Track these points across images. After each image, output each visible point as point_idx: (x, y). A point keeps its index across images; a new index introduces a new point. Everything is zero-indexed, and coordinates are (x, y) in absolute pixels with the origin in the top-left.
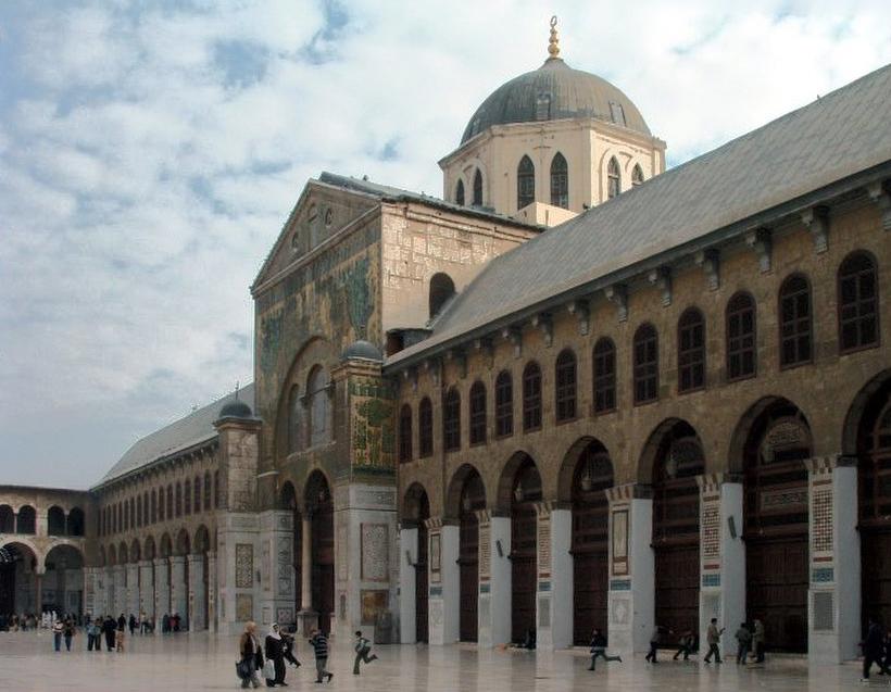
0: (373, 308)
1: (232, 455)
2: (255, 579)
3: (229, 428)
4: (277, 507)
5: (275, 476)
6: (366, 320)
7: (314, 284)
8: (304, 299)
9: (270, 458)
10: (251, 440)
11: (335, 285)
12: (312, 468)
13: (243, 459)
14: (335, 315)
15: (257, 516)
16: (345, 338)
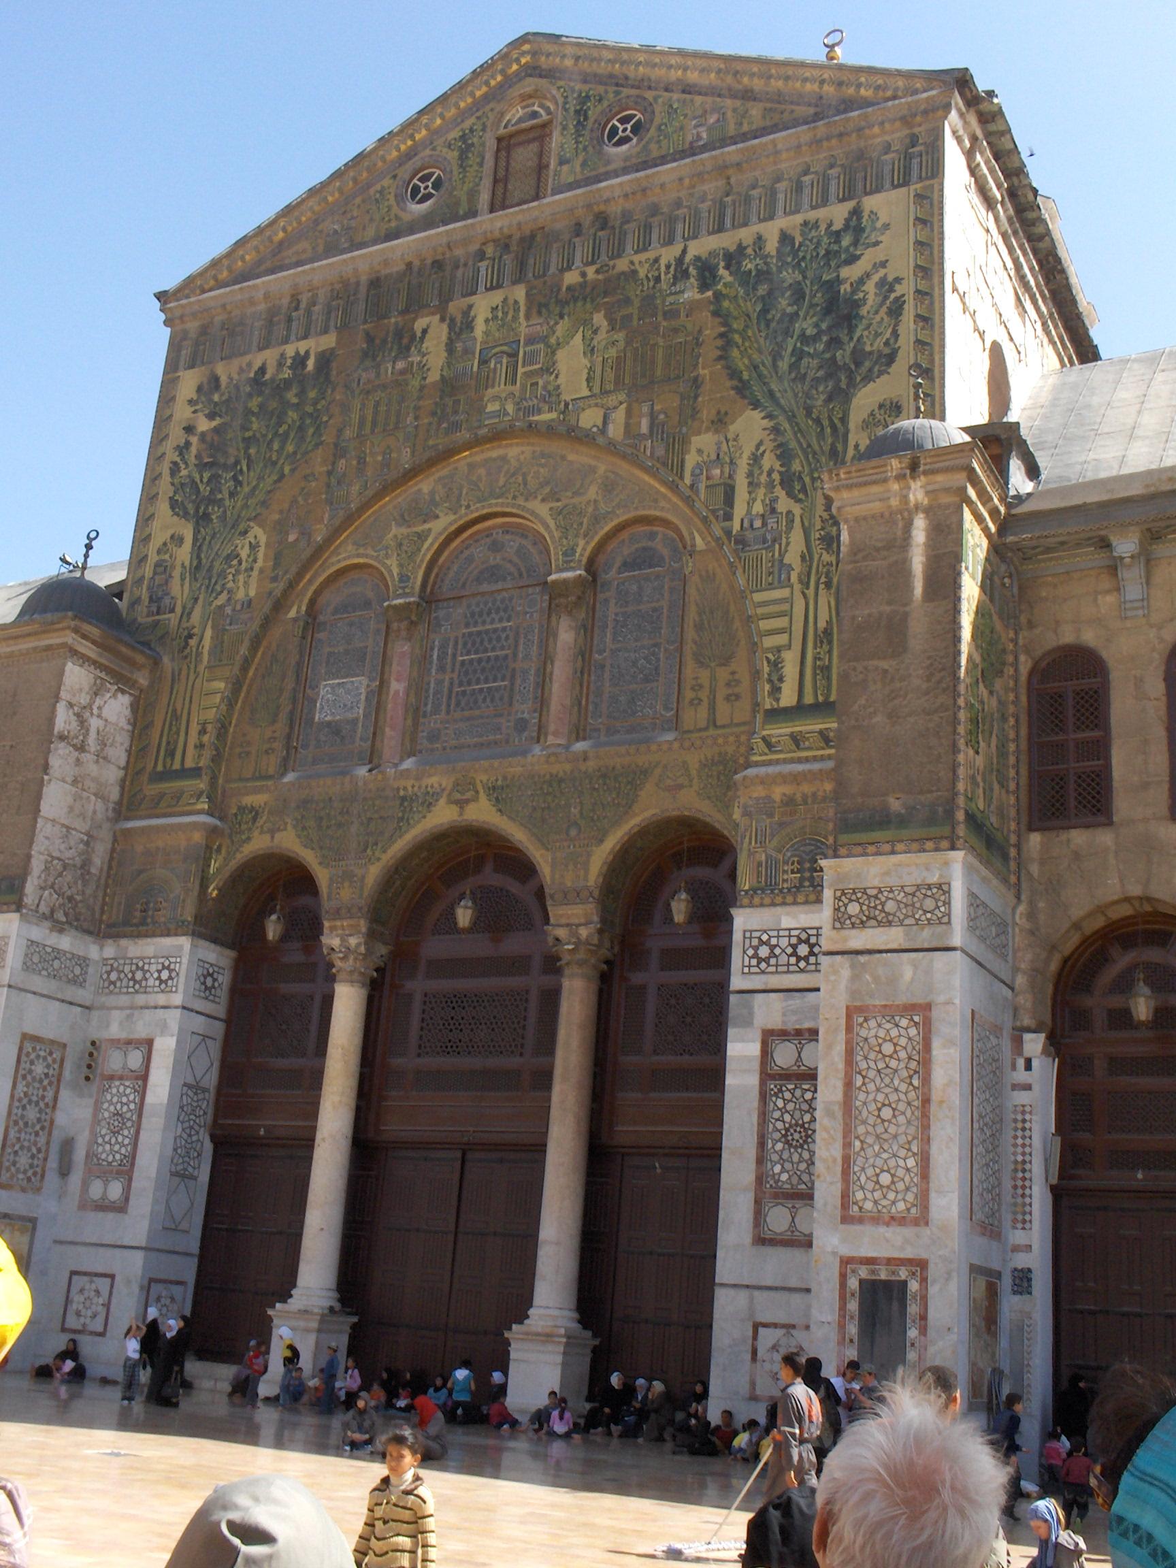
0: (891, 358)
1: (62, 738)
2: (53, 1163)
3: (74, 653)
4: (206, 927)
5: (213, 831)
6: (842, 396)
7: (520, 293)
8: (461, 327)
9: (196, 772)
10: (116, 709)
11: (648, 302)
12: (443, 816)
13: (85, 757)
14: (633, 375)
15: (94, 951)
16: (703, 443)
